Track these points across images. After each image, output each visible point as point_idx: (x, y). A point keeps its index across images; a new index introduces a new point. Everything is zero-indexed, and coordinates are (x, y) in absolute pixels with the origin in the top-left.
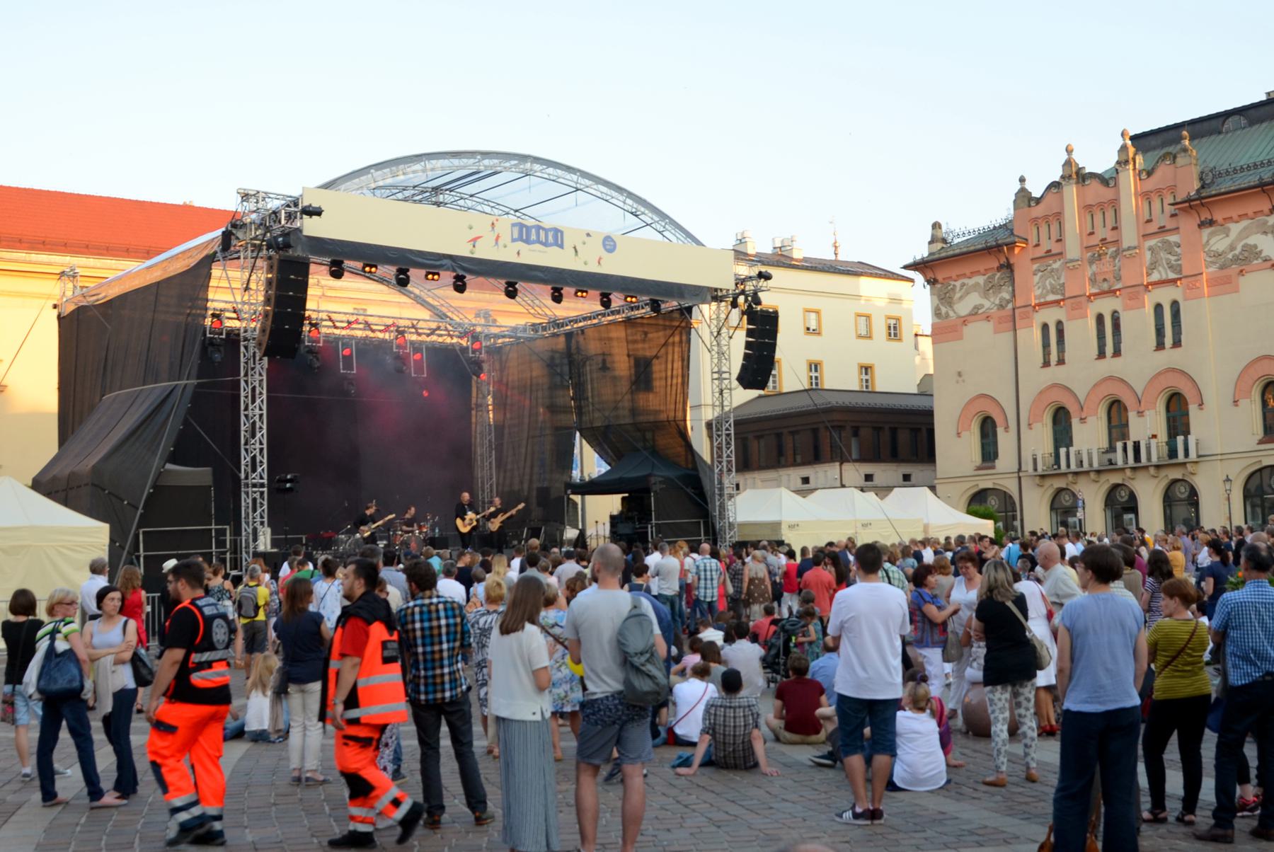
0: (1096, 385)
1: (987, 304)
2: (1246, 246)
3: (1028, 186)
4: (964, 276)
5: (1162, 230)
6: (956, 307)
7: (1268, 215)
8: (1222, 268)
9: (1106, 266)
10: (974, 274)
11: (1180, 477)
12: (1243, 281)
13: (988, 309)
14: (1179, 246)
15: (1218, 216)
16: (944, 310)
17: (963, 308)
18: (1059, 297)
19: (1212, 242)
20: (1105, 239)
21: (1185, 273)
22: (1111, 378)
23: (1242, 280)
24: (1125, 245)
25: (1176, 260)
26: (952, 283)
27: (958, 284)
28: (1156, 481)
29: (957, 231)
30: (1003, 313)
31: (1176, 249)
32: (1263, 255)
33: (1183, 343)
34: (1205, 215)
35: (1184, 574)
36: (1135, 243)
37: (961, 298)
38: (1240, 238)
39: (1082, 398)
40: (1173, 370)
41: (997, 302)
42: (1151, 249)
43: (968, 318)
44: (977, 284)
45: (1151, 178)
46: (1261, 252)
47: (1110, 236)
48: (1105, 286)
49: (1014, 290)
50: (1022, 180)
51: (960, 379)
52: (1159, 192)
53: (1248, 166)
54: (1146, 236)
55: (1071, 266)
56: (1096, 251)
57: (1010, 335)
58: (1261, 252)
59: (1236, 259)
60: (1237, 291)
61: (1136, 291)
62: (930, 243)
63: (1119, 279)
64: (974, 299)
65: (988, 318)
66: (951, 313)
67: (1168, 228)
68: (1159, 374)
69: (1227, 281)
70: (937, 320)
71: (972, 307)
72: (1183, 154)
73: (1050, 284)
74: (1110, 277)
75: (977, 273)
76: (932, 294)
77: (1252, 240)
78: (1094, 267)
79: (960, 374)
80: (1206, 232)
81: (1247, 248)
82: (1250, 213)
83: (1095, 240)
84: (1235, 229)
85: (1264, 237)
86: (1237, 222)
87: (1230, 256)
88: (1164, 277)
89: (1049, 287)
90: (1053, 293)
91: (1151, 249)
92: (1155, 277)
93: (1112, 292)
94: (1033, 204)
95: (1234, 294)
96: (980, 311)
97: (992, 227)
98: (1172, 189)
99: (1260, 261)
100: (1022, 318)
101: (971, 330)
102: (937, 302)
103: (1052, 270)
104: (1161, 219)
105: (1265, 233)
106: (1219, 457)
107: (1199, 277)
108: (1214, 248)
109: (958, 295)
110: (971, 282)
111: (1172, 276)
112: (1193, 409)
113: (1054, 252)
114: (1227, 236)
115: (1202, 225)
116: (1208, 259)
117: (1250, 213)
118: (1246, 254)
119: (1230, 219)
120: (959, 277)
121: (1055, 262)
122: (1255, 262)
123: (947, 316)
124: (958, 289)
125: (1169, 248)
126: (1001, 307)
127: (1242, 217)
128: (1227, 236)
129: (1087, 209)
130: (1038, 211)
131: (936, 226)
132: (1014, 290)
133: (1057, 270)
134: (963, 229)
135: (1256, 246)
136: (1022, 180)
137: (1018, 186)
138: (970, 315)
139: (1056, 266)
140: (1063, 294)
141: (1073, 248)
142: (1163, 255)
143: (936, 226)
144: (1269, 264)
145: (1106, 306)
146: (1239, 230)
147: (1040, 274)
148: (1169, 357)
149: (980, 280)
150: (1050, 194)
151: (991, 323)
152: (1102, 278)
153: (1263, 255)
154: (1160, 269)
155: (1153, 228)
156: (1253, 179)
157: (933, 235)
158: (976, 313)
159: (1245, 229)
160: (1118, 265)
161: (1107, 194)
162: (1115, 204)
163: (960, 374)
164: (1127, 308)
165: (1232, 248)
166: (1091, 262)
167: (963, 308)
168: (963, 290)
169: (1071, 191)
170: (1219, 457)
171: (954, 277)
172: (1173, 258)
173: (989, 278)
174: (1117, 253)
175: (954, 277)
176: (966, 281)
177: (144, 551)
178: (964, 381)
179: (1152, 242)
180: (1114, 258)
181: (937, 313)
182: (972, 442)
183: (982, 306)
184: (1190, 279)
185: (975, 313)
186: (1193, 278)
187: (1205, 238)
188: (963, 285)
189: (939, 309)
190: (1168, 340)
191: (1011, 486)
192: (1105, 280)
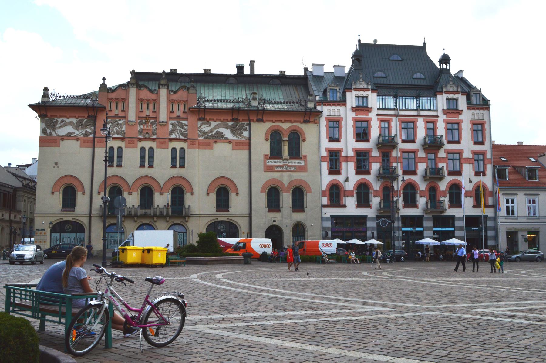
0: (139, 179)
1: (77, 132)
2: (218, 131)
3: (106, 82)
4: (66, 117)
5: (178, 118)
6: (56, 131)
7: (229, 122)
8: (206, 138)
9: (148, 127)
10: (70, 117)
11: (180, 223)
12: (215, 145)
13: (78, 135)
14: (187, 126)
15: (207, 117)
16: (48, 131)
17: (62, 132)
18: (121, 136)
19: (203, 127)
20: (149, 115)
21: (188, 138)
22: (147, 176)
23: (215, 145)
24: (161, 120)
25: (184, 131)
26: (56, 119)
27: (60, 120)
28: (167, 224)
29: (60, 94)
30: (86, 138)
31: (185, 127)
32: (225, 137)
33: (186, 166)
34: (202, 116)
35: (377, 268)
36: (165, 120)
37: (61, 127)
38: (215, 127)
39: (130, 183)
40: (180, 177)
41: (84, 132)
42: (172, 124)
43: (65, 138)
44: (72, 122)
45: (174, 95)
46: (224, 135)
47: (151, 115)
48: (147, 136)
49: (95, 129)
50: (104, 79)
51: (56, 166)
52: (179, 102)
53: (218, 100)
54: (171, 119)
55: (128, 123)
56: (144, 120)
57: (90, 150)
58: (224, 135)
59: (212, 136)
60: (212, 149)
61: (163, 142)
62: (43, 97)
63: (154, 134)
64: (69, 129)
65: (78, 140)
66: (53, 133)
67: (181, 117)
68: (173, 177)
69: (208, 144)
70: (44, 135)
71: (67, 132)
72: (192, 88)
73: (116, 129)
74: (150, 132)
75: (74, 117)
76: (41, 121)
77: (221, 130)
78: (142, 126)
79: (56, 164)
80: (199, 123)
81: (217, 132)
82: (222, 119)
83: (143, 115)
84: (213, 124)
85: (226, 130)
86: (215, 121)
87: (210, 134)
88: (178, 137)
89: (115, 131)
90: (118, 134)
91: (172, 124)
92: (173, 136)
93: (149, 139)
94: (110, 91)
95: (211, 150)
96: (72, 135)
97: (72, 96)
98: (186, 102)
99: (223, 139)
100: (98, 143)
101: (65, 144)
102: (44, 126)
103: (118, 124)
104: (177, 113)
105: (227, 128)
106: (199, 216)
107: (196, 140)
108: (203, 130)
109: (58, 125)
110: (68, 120)
111: (181, 137)
112: (188, 195)
113: (119, 115)
114: (210, 126)
115: (200, 119)
116: (200, 133)
117: (222, 119)
118: (218, 135)
119: (210, 119)
120: (61, 117)
121: (120, 120)
122: (221, 139)
123: (51, 134)
124: (59, 122)
125: (181, 126)
126: (87, 134)
127: (217, 120)
128: (210, 126)
129: (140, 101)
130: (113, 96)
131: (46, 89)
132: (95, 129)
133: (121, 124)
134: (64, 94)
135: (222, 133)
136: (104, 79)
137: (102, 82)
138: (66, 136)
139: (119, 122)
140: (123, 135)
141: (132, 116)
142: (178, 128)
143: (46, 89)
144: (228, 141)
145: (147, 145)
146: (214, 125)
147: (111, 124)
148: (177, 171)
149: (75, 120)
150: (120, 89)
151: (79, 142)
152: (146, 132)
153: (225, 137)
154: (176, 133)
155: (174, 115)
156: (229, 105)
157: (44, 93)
158: (70, 136)
159: (218, 125)
160: (155, 128)
161: (152, 96)
162: (156, 102)
163: (56, 164)
164: (157, 147)
165: (211, 131)
166: (140, 124)
167: (62, 132)
168: (62, 124)
169: (133, 91)
170: (199, 216)
171: (58, 116)
172: (183, 130)
173: (79, 120)
174: (155, 122)
175: (58, 116)
176: (65, 119)
177: (482, 249)
178: (58, 167)
179: (173, 122)
180: (153, 125)
181: (44, 131)
182: (58, 198)
183: (74, 133)
184: (191, 140)
185: (69, 136)
186: (194, 140)
187: (199, 126)
188: (62, 121)
189: (46, 130)
190: (178, 165)
191: (85, 221)
192: (147, 133)
